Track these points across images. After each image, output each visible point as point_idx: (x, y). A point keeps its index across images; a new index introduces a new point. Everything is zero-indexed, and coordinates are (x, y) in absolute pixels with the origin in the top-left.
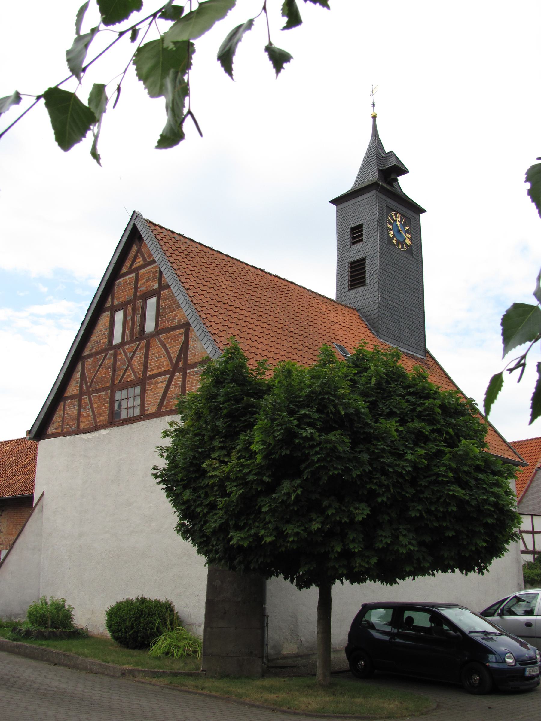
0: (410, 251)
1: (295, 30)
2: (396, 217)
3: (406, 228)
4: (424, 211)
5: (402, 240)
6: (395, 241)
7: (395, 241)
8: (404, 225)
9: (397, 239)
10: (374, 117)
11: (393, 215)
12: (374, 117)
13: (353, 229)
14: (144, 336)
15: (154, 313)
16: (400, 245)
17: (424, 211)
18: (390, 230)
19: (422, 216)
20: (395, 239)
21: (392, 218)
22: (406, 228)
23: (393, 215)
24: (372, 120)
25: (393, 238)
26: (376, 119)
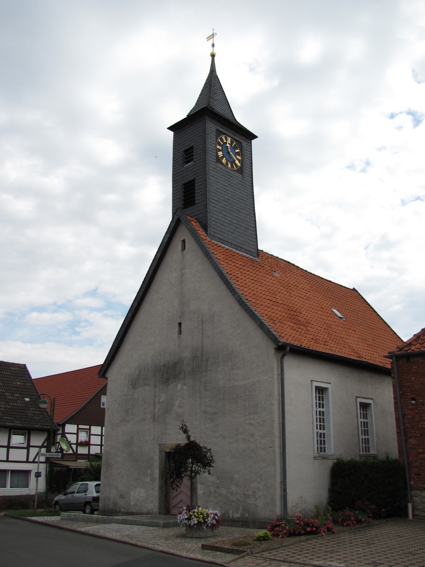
0: (241, 170)
1: (421, 125)
2: (227, 140)
3: (237, 151)
4: (255, 137)
5: (231, 160)
6: (224, 161)
7: (224, 161)
8: (235, 148)
9: (226, 159)
10: (213, 56)
11: (223, 138)
12: (213, 56)
13: (185, 151)
14: (12, 434)
15: (212, 553)
16: (229, 165)
17: (255, 137)
18: (219, 150)
19: (253, 141)
20: (224, 159)
21: (222, 140)
22: (237, 151)
23: (223, 138)
24: (211, 58)
25: (222, 158)
26: (215, 58)
